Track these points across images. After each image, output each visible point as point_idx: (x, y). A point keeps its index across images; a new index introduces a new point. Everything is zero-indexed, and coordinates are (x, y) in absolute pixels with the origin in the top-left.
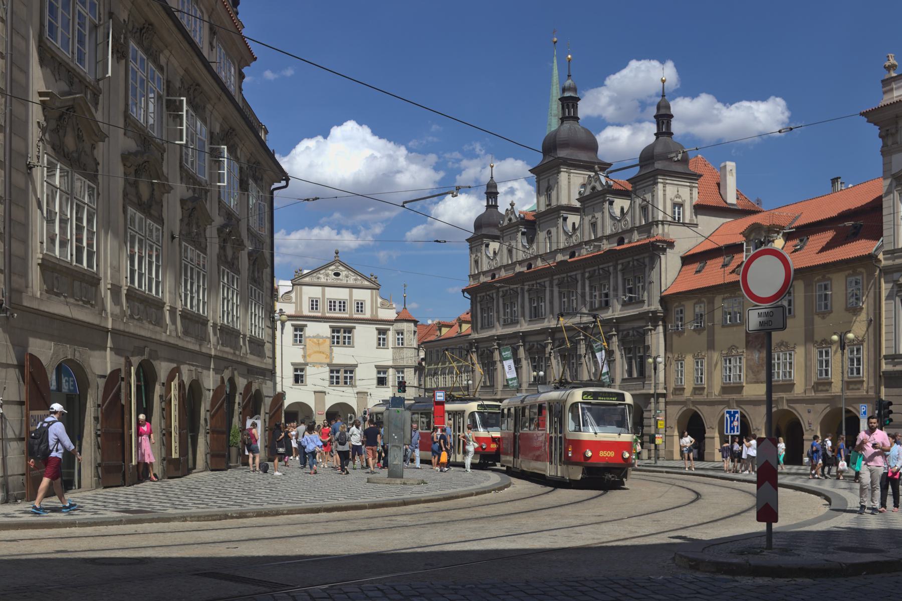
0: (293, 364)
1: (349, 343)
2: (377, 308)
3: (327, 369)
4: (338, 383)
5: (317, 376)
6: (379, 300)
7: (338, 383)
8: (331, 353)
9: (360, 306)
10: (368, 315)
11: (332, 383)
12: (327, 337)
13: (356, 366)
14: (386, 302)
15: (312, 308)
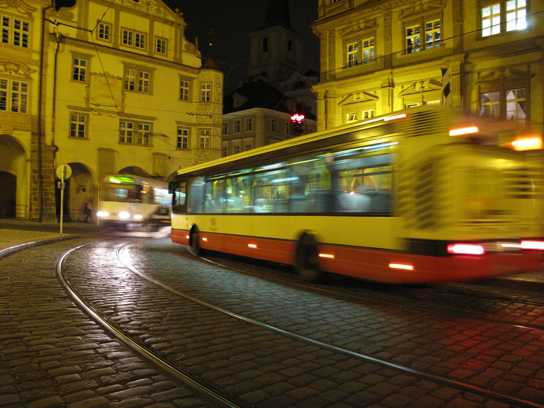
0: (69, 107)
1: (146, 90)
2: (181, 52)
3: (116, 121)
4: (130, 140)
5: (104, 130)
6: (184, 42)
7: (130, 140)
8: (123, 100)
9: (161, 46)
10: (171, 56)
11: (122, 140)
12: (119, 78)
13: (154, 119)
14: (192, 46)
15: (101, 36)
